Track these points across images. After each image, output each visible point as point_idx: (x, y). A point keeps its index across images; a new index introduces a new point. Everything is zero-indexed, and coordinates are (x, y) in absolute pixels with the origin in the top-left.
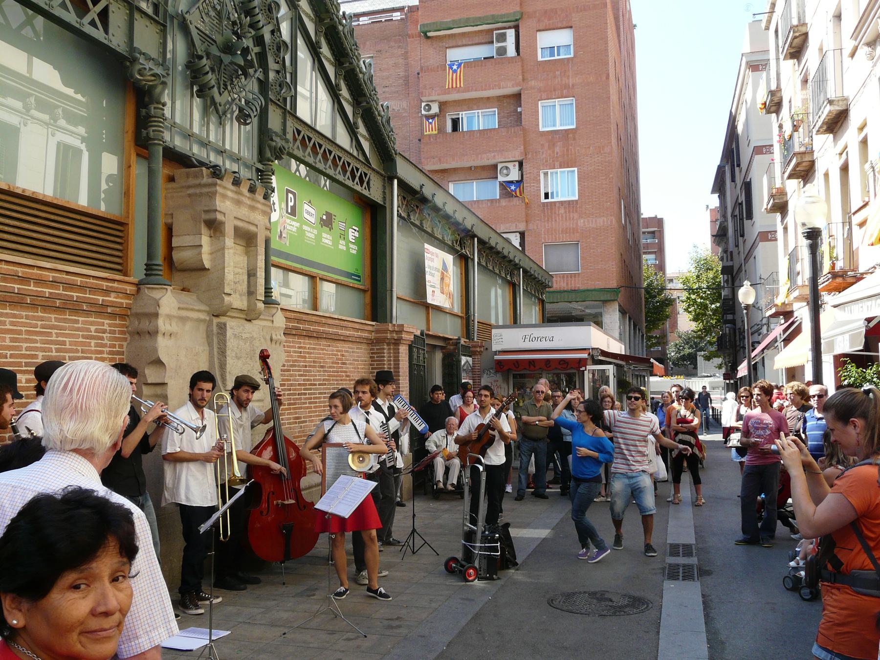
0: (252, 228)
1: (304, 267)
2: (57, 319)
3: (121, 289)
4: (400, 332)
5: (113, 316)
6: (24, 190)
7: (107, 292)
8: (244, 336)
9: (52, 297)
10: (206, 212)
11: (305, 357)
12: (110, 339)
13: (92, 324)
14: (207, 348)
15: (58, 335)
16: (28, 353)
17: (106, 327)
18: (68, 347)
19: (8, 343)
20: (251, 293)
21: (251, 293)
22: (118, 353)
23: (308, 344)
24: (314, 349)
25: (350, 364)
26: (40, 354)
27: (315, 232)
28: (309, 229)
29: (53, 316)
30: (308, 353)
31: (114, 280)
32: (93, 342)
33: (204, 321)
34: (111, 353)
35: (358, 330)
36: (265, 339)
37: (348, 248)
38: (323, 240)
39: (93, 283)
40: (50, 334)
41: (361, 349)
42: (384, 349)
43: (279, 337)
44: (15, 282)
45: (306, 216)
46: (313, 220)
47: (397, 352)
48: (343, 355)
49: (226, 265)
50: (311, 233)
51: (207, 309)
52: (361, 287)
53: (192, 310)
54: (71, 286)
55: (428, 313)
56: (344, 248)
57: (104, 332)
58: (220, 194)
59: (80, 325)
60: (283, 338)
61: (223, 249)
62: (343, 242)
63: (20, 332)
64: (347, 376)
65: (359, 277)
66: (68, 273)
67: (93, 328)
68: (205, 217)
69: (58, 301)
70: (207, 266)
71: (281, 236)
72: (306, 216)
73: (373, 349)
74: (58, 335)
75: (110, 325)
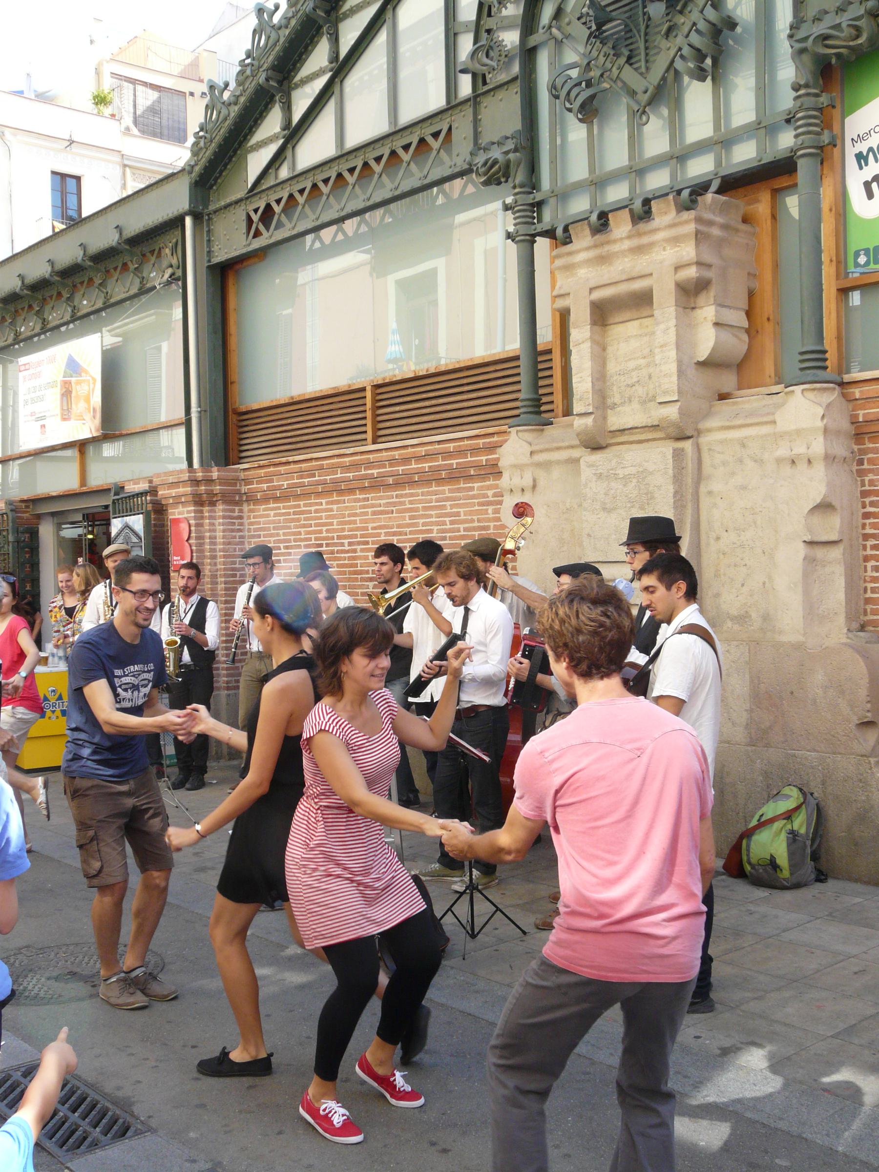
0: (637, 285)
2: (450, 491)
8: (621, 473)
13: (489, 488)
15: (452, 506)
16: (424, 528)
18: (462, 517)
26: (435, 528)
29: (446, 488)
36: (759, 462)
39: (467, 445)
44: (399, 464)
54: (447, 455)
58: (559, 268)
59: (475, 492)
66: (439, 442)
67: (490, 493)
69: (444, 473)
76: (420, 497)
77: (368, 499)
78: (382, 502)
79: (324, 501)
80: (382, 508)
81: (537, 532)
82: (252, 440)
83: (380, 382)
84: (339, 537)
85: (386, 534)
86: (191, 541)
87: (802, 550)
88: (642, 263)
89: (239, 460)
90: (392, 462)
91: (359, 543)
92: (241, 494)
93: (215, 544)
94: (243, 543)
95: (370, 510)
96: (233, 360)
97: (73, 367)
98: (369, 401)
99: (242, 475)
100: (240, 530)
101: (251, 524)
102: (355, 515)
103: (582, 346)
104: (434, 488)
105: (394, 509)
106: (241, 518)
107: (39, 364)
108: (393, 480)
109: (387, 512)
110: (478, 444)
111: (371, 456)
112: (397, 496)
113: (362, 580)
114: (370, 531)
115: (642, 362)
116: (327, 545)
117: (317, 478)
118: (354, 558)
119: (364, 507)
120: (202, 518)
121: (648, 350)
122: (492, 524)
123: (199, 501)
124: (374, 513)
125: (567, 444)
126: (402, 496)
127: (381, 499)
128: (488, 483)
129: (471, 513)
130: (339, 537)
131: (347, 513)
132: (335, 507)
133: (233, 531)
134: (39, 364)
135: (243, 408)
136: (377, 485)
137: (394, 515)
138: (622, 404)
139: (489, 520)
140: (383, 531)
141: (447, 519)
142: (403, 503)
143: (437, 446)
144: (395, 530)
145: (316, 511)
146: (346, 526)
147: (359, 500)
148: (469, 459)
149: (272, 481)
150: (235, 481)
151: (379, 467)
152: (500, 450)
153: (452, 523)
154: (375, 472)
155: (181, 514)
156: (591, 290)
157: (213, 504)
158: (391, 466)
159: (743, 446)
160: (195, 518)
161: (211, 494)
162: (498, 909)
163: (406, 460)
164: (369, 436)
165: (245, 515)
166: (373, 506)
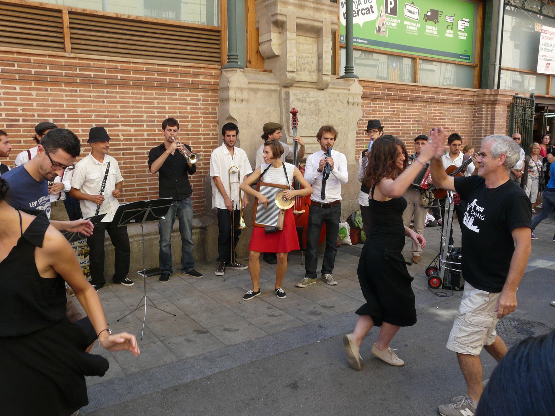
1: (404, 52)
3: (206, 72)
4: (496, 95)
5: (205, 90)
6: (129, 16)
7: (196, 75)
10: (273, 15)
11: (399, 115)
12: (204, 105)
13: (187, 95)
14: (278, 108)
16: (135, 114)
17: (200, 97)
18: (167, 110)
19: (119, 109)
20: (319, 70)
21: (319, 70)
22: (211, 113)
23: (401, 105)
24: (409, 109)
25: (450, 119)
26: (145, 115)
27: (418, 25)
28: (411, 24)
29: (154, 92)
30: (402, 112)
31: (200, 68)
32: (189, 107)
33: (275, 91)
34: (204, 113)
35: (457, 95)
36: (342, 102)
37: (456, 36)
38: (427, 31)
41: (463, 108)
42: (482, 108)
43: (357, 100)
45: (407, 14)
46: (416, 17)
47: (493, 110)
48: (441, 113)
49: (288, 52)
50: (413, 27)
51: (279, 82)
52: (471, 64)
53: (263, 83)
55: (548, 81)
56: (452, 36)
57: (199, 100)
59: (177, 97)
60: (361, 101)
61: (286, 40)
62: (451, 31)
63: (129, 102)
64: (445, 128)
65: (469, 56)
66: (158, 65)
67: (188, 98)
68: (273, 19)
70: (277, 54)
71: (379, 30)
72: (407, 14)
73: (475, 109)
74: (158, 103)
75: (203, 96)
76: (131, 95)
77: (76, 91)
78: (92, 94)
79: (18, 87)
80: (92, 99)
81: (251, 121)
83: (79, 11)
87: (356, 135)
88: (317, 15)
90: (110, 70)
91: (66, 121)
95: (78, 99)
102: (62, 101)
103: (292, 41)
104: (143, 91)
105: (105, 100)
108: (108, 82)
109: (99, 102)
111: (92, 63)
112: (107, 92)
114: (79, 113)
115: (309, 55)
117: (16, 68)
119: (71, 96)
121: (311, 51)
122: (190, 116)
125: (268, 82)
126: (113, 92)
127: (92, 93)
128: (186, 93)
129: (174, 108)
131: (50, 98)
132: (34, 93)
136: (87, 82)
137: (105, 104)
138: (300, 70)
139: (188, 113)
140: (93, 114)
141: (155, 110)
143: (156, 67)
144: (106, 113)
146: (50, 109)
147: (65, 91)
148: (179, 78)
151: (97, 71)
154: (92, 74)
156: (297, 17)
158: (108, 72)
159: (338, 96)
166: (81, 96)
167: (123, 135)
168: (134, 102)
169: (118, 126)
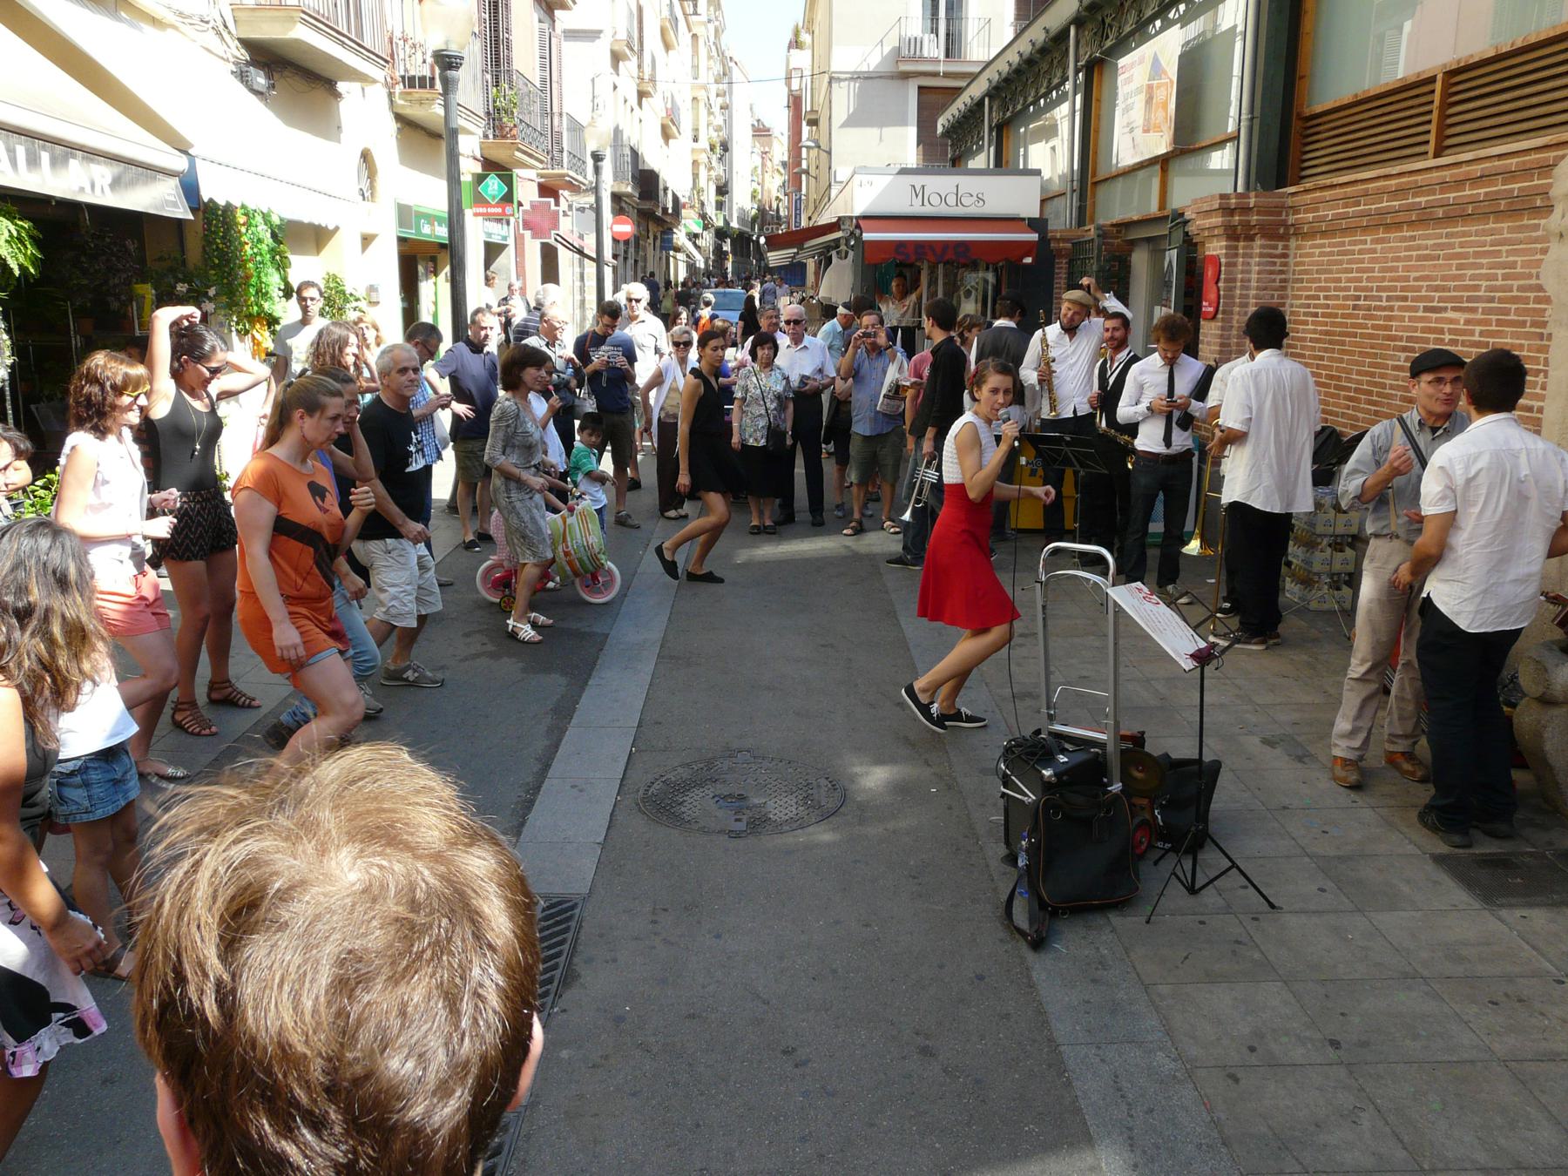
9: (1492, 198)
26: (1484, 284)
29: (1505, 225)
40: (1497, 254)
54: (1510, 176)
66: (1500, 156)
77: (1413, 238)
78: (1430, 242)
82: (1321, 150)
84: (1379, 289)
85: (1430, 288)
86: (1221, 284)
89: (1299, 180)
90: (1444, 186)
92: (1287, 227)
93: (1248, 288)
94: (1284, 288)
96: (1305, 45)
97: (1157, 68)
98: (1437, 97)
99: (1290, 201)
100: (1281, 272)
101: (1297, 264)
102: (1397, 259)
106: (1285, 256)
107: (1132, 65)
110: (1547, 159)
113: (1395, 348)
116: (1366, 298)
118: (1390, 318)
119: (1408, 249)
120: (1236, 255)
123: (1232, 234)
124: (1419, 258)
127: (1428, 238)
130: (1379, 289)
133: (1272, 273)
134: (1132, 65)
135: (1307, 112)
136: (1425, 219)
141: (1500, 272)
142: (1451, 246)
145: (1360, 252)
147: (1404, 239)
149: (1316, 210)
150: (1279, 209)
152: (1556, 171)
153: (1505, 277)
155: (1216, 248)
157: (1251, 238)
160: (1227, 255)
161: (1247, 225)
162: (1234, 865)
163: (1459, 184)
164: (1431, 148)
165: (1291, 253)
166: (1419, 248)
167: (1451, 331)
168: (1477, 255)
169: (1445, 309)
